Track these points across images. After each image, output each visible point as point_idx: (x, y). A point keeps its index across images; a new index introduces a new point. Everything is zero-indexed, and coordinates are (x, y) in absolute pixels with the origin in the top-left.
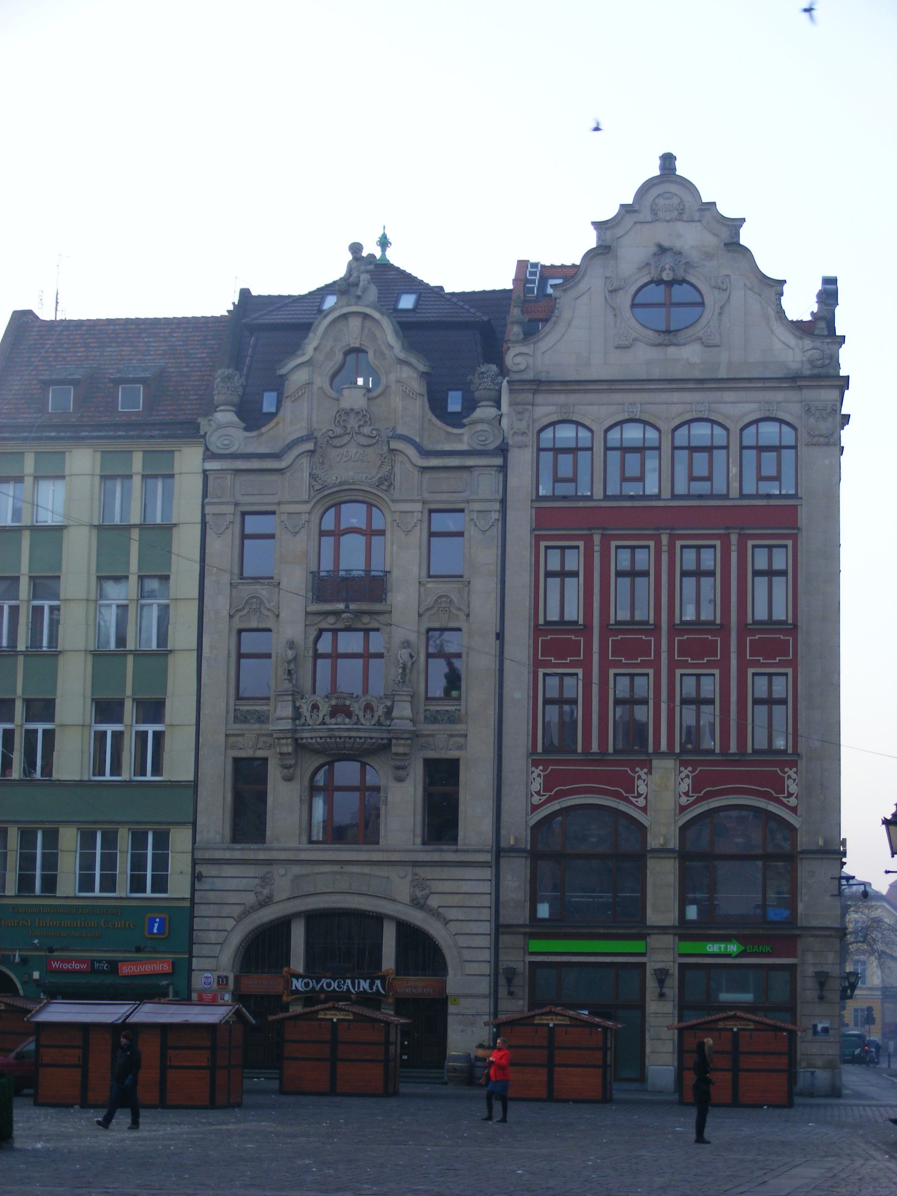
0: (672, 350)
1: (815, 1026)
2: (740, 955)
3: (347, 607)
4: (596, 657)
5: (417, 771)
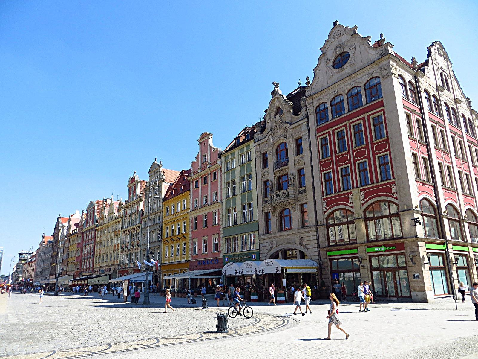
0: (343, 72)
1: (414, 275)
2: (385, 251)
4: (335, 164)
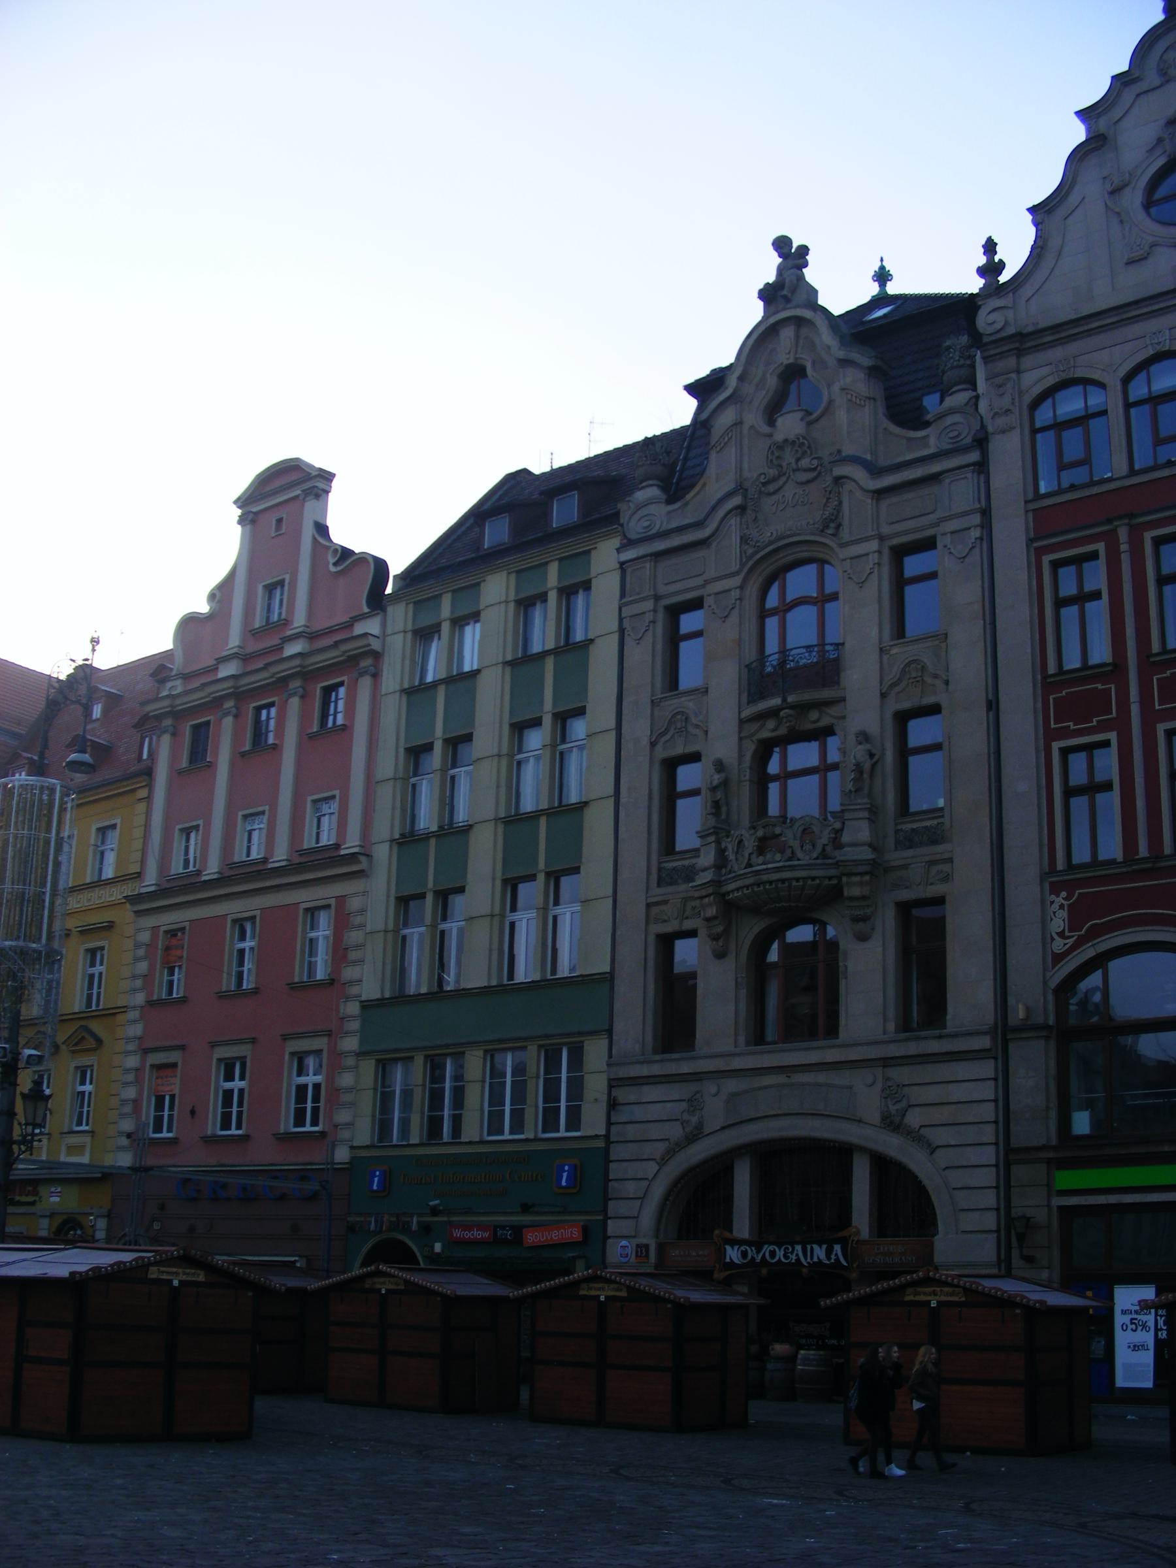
3: (784, 700)
4: (1135, 709)
5: (887, 921)
